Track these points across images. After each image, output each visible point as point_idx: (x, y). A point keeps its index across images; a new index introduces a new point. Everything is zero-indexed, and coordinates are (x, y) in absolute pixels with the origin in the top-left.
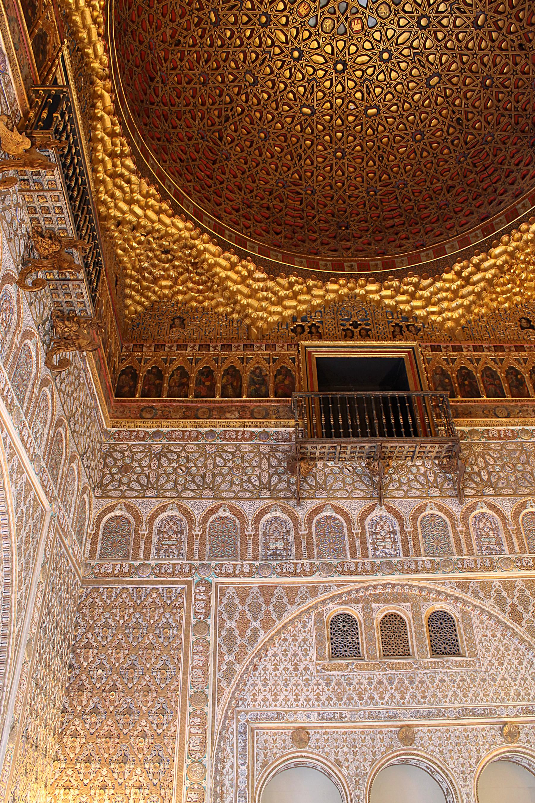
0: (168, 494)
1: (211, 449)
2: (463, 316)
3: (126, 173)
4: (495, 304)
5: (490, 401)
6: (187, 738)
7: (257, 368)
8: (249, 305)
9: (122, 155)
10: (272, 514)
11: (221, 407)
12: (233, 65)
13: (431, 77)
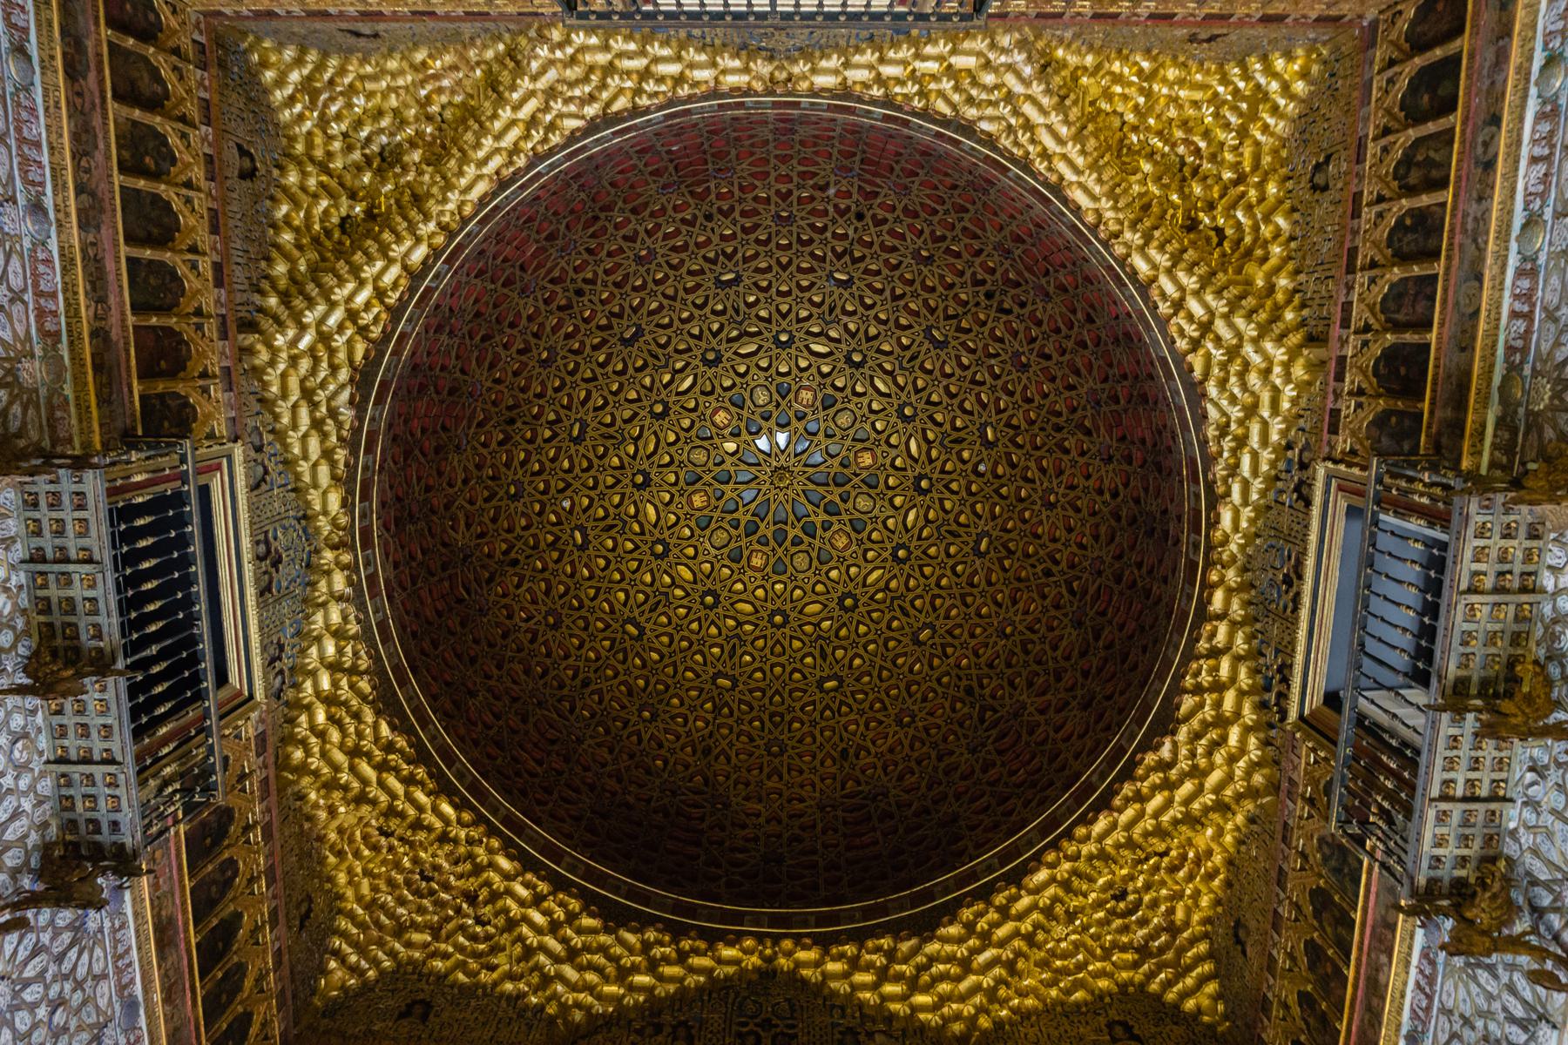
2: (1279, 340)
3: (920, 959)
4: (1276, 250)
5: (1442, 325)
7: (1320, 848)
8: (1218, 790)
9: (891, 955)
11: (1368, 979)
12: (900, 661)
13: (933, 340)
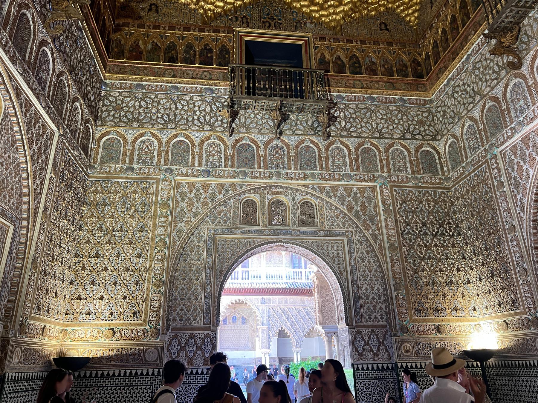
0: (463, 114)
1: (470, 69)
6: (513, 254)
10: (512, 84)
